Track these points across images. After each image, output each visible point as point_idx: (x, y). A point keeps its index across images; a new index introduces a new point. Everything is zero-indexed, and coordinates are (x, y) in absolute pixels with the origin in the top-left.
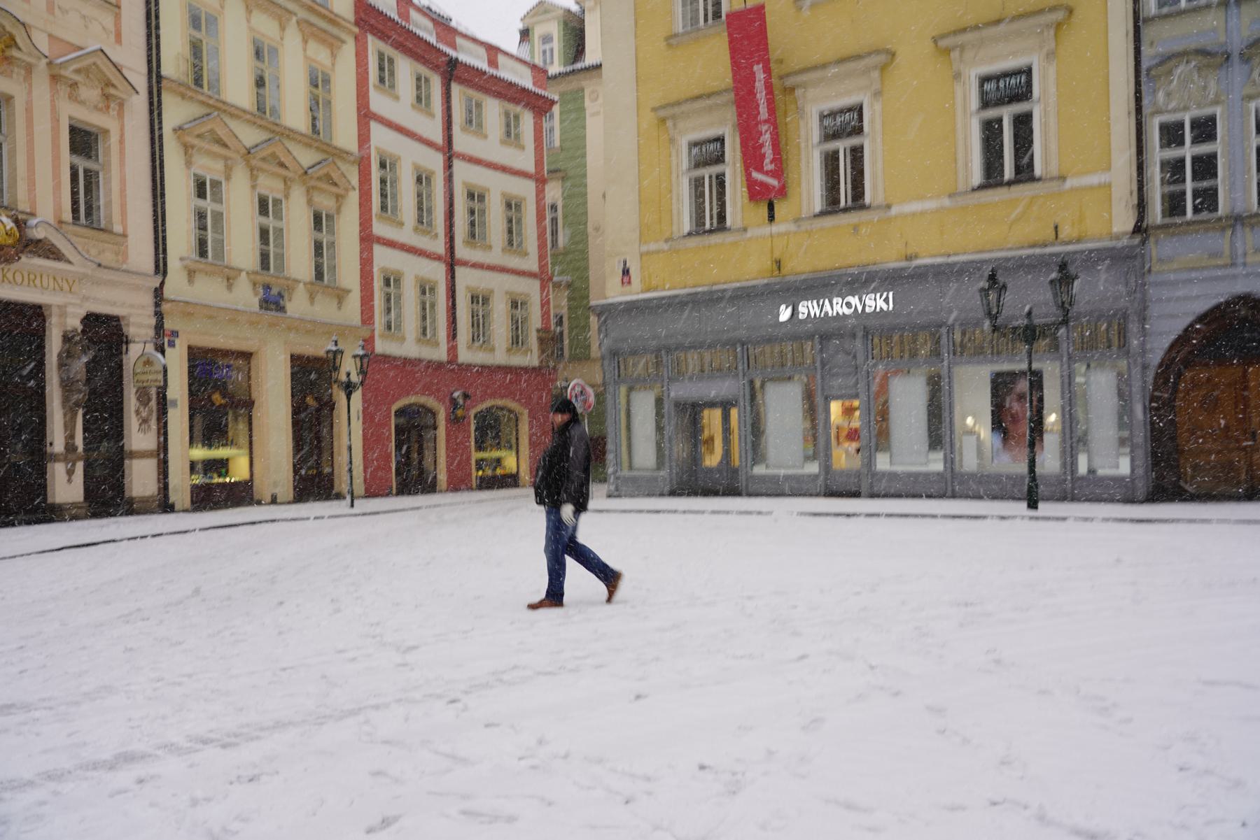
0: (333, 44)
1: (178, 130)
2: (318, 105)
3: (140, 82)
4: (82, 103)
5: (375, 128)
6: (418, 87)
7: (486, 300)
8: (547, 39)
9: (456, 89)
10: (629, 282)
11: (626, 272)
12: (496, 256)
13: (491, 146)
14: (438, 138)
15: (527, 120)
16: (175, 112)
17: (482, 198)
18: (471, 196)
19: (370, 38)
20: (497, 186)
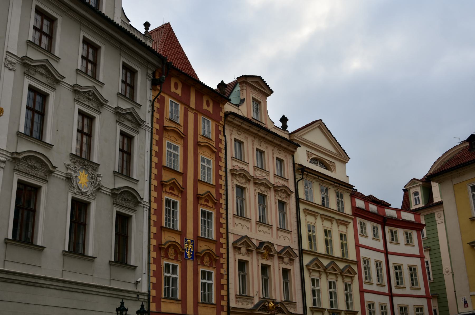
0: (346, 224)
1: (306, 266)
2: (344, 246)
3: (297, 252)
4: (284, 263)
5: (362, 250)
6: (374, 231)
7: (406, 309)
8: (416, 194)
9: (387, 228)
10: (467, 306)
11: (466, 302)
12: (408, 291)
13: (402, 247)
14: (382, 248)
15: (414, 234)
16: (307, 260)
17: (400, 268)
18: (396, 268)
19: (357, 218)
20: (405, 262)
